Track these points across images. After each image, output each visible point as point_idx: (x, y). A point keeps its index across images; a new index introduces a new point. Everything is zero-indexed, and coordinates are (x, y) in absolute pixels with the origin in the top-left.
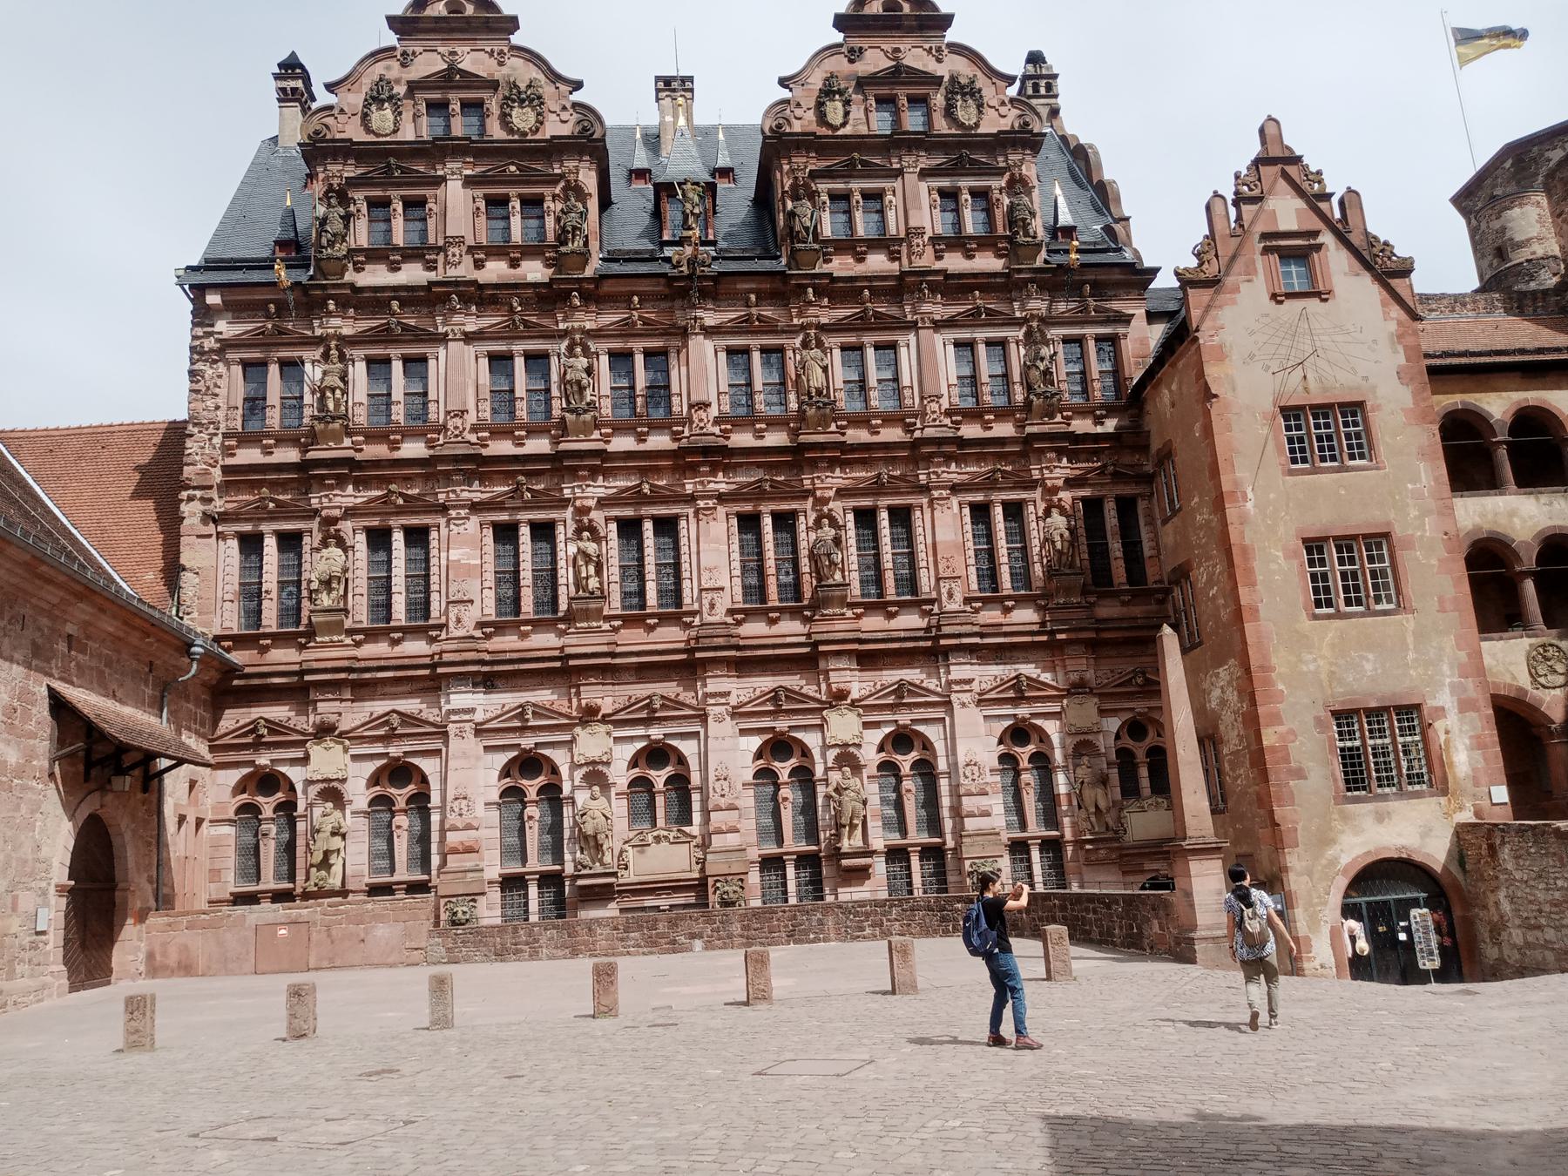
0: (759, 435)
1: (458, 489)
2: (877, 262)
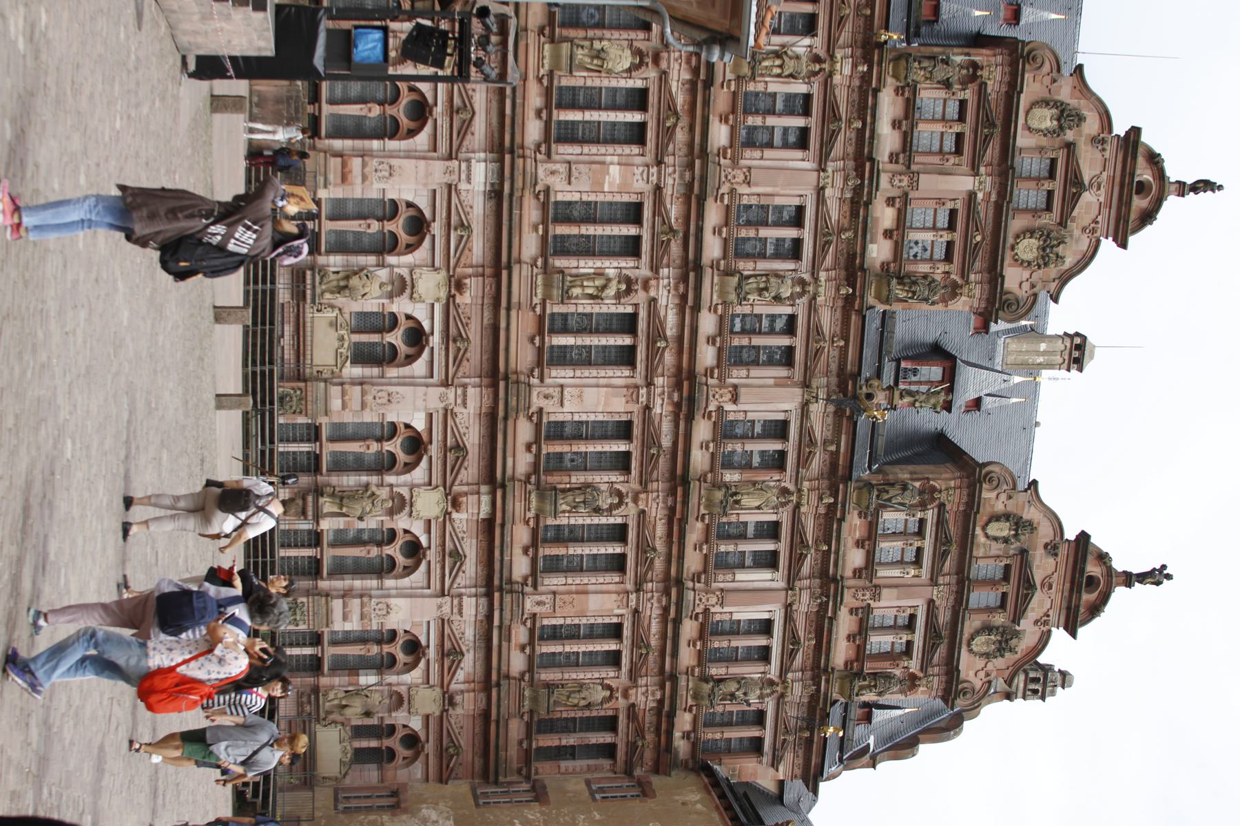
0: (704, 446)
1: (676, 176)
2: (855, 558)
